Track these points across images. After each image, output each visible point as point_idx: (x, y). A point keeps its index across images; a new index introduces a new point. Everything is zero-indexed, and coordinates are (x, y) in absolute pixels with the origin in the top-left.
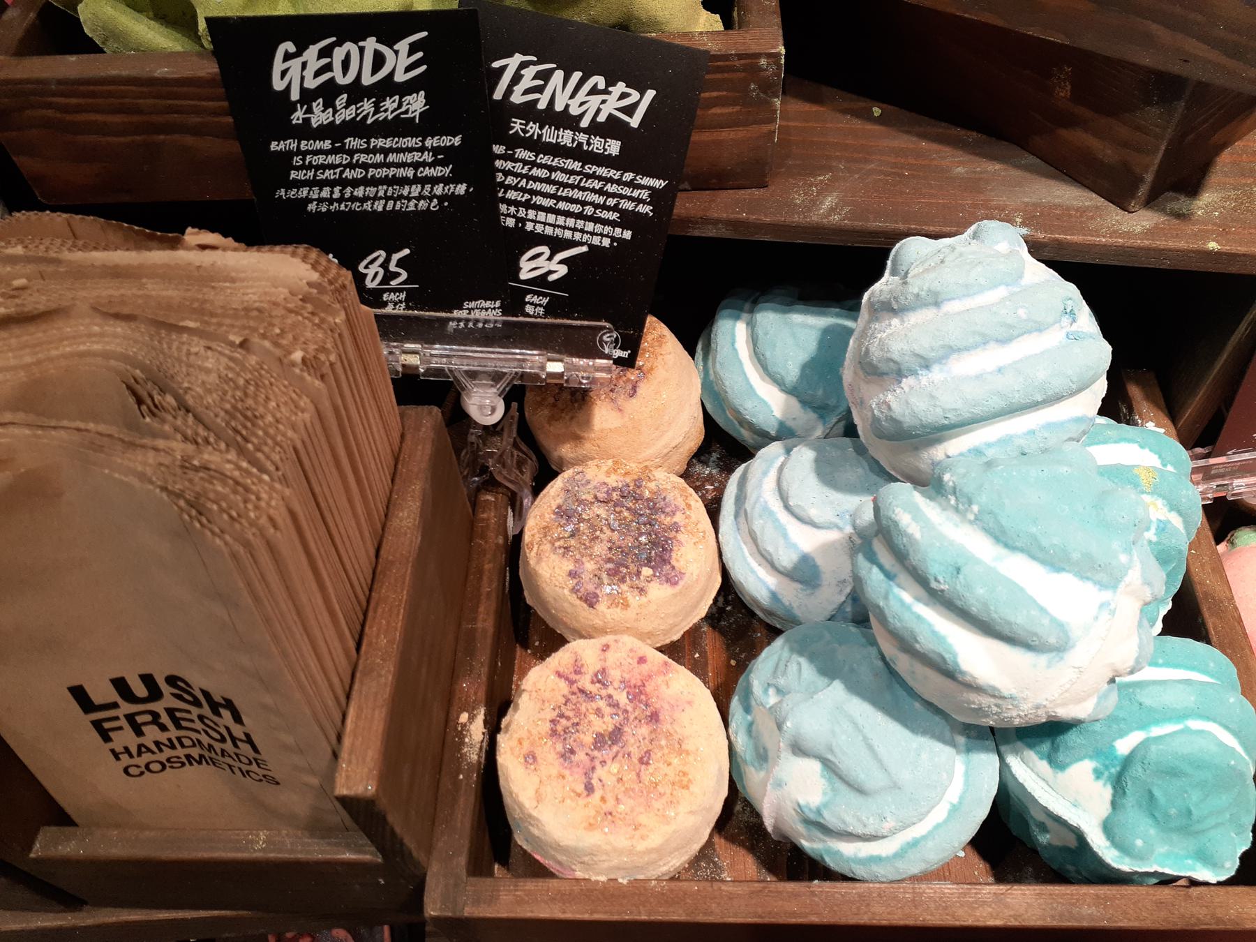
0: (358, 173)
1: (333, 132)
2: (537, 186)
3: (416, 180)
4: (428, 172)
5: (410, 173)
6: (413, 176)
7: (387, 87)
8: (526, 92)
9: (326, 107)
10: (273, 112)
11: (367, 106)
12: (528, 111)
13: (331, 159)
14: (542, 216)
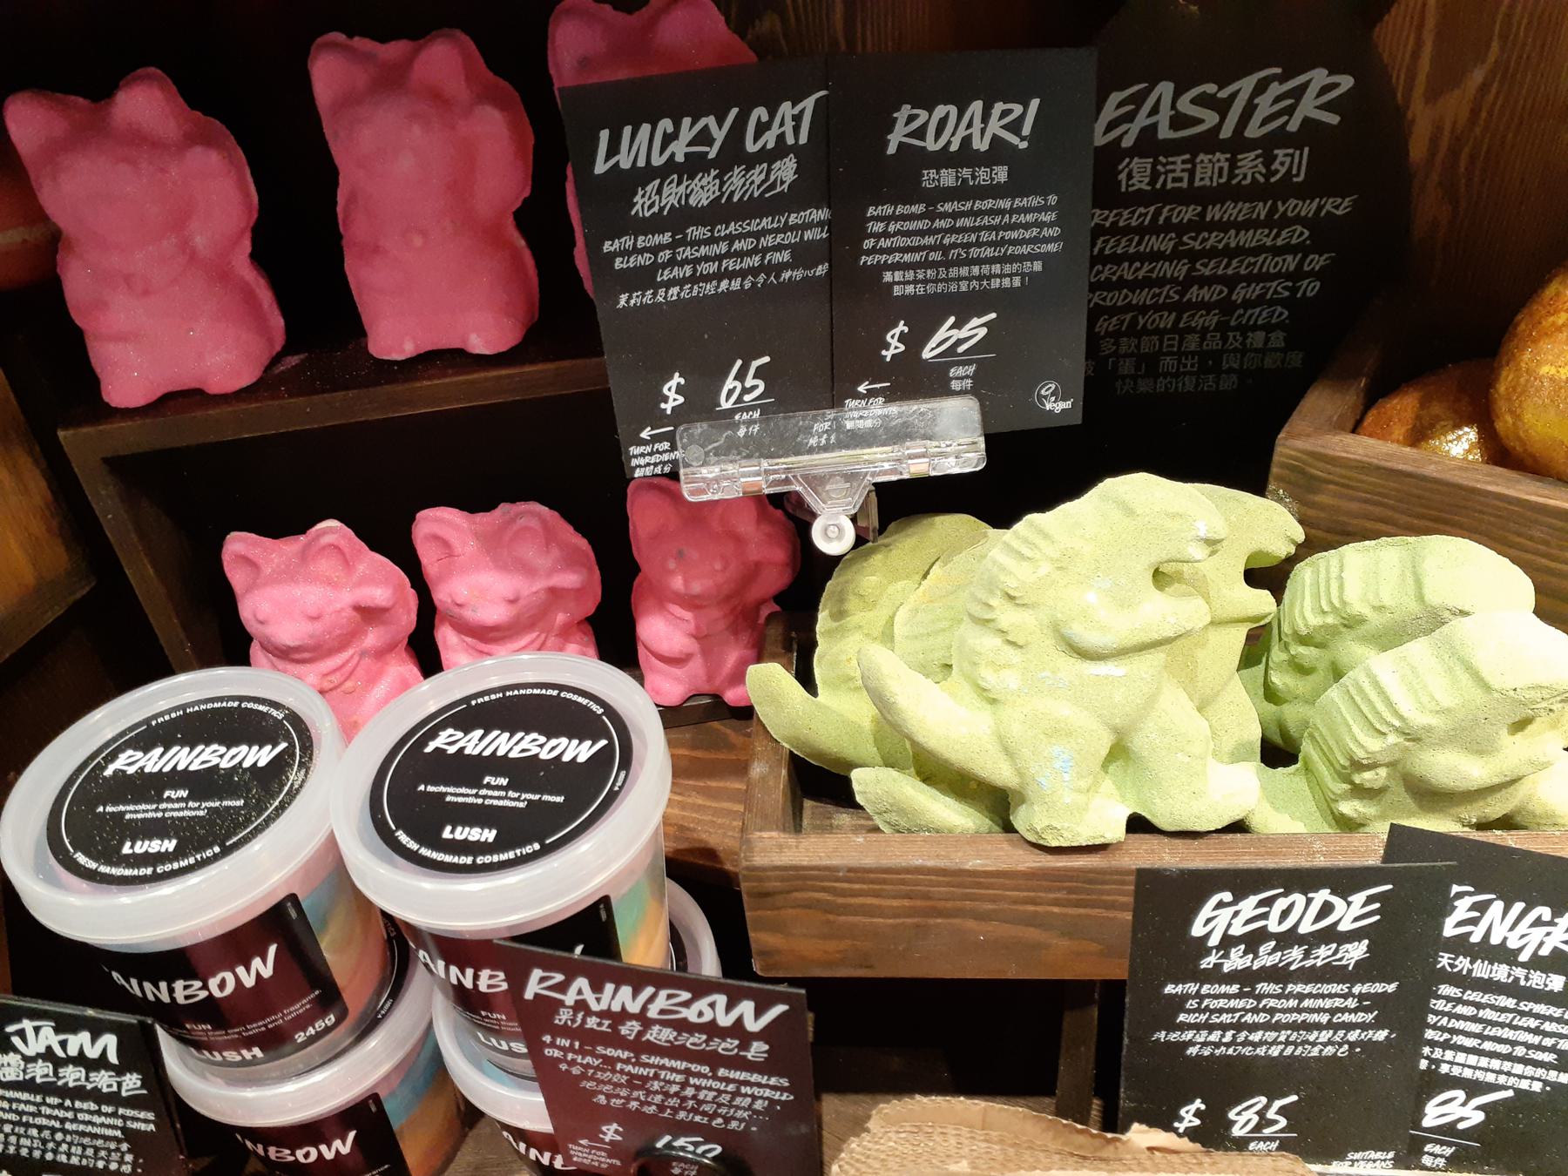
0: (1262, 1018)
1: (1246, 978)
2: (1460, 1025)
3: (1330, 1025)
4: (1346, 1017)
5: (1324, 1018)
6: (1330, 1024)
7: (1331, 935)
8: (1459, 924)
9: (1246, 953)
10: (1186, 957)
11: (1296, 953)
12: (1460, 945)
13: (1233, 1003)
14: (1461, 1057)
